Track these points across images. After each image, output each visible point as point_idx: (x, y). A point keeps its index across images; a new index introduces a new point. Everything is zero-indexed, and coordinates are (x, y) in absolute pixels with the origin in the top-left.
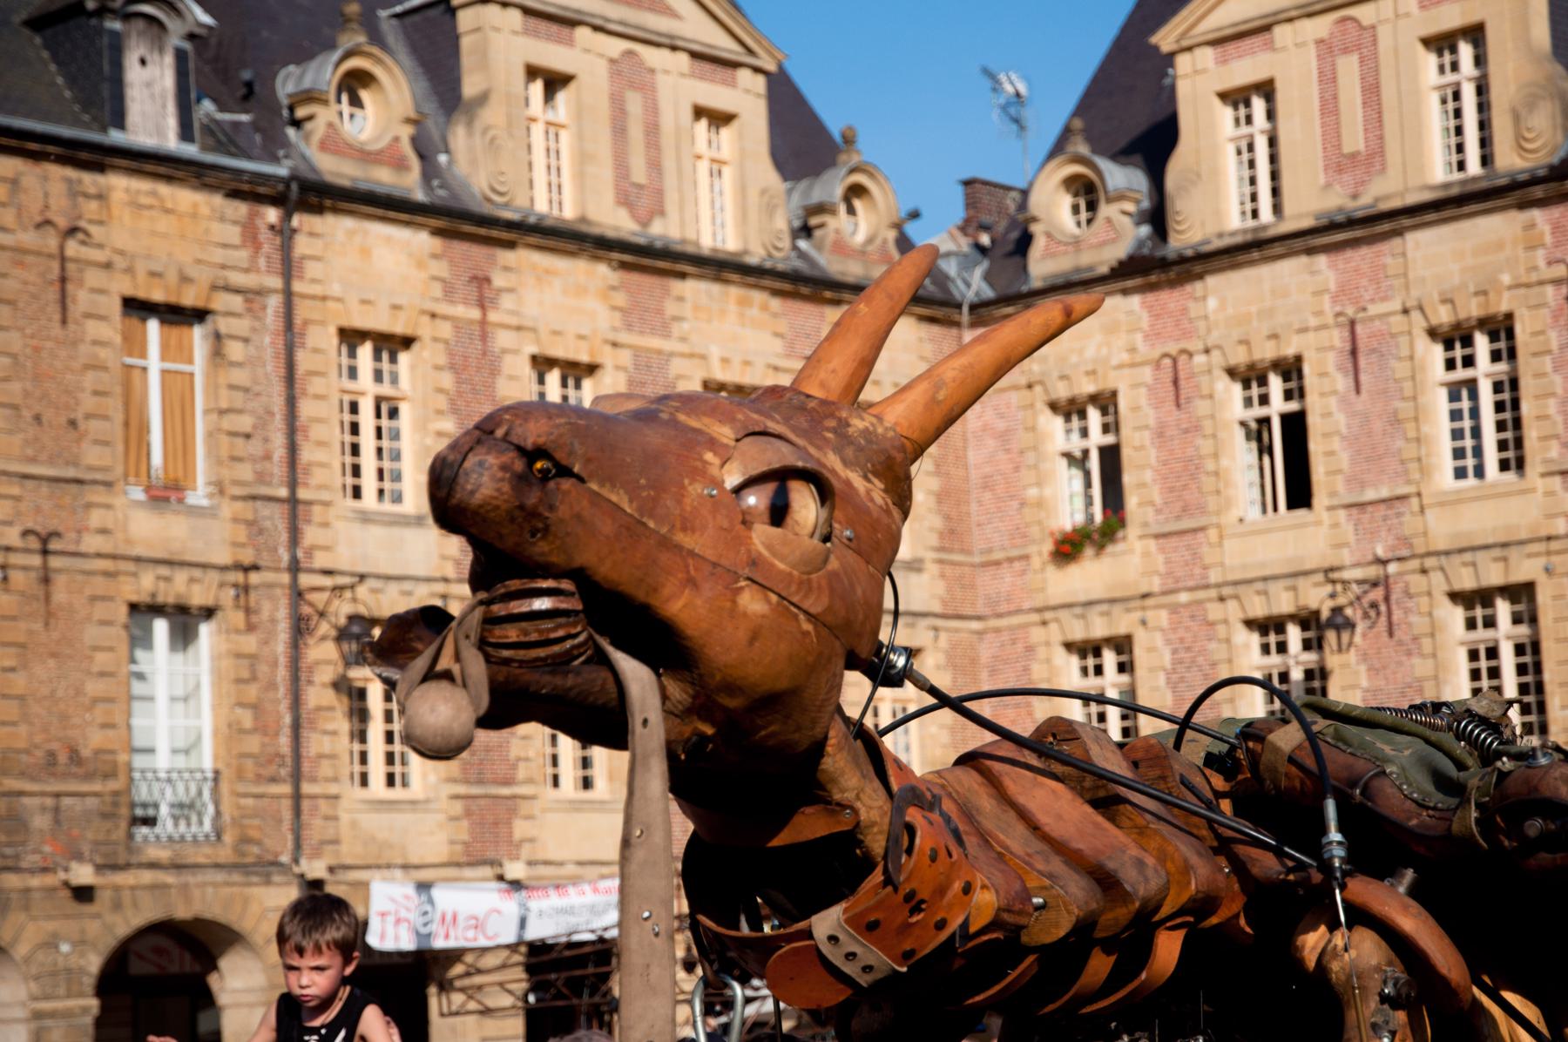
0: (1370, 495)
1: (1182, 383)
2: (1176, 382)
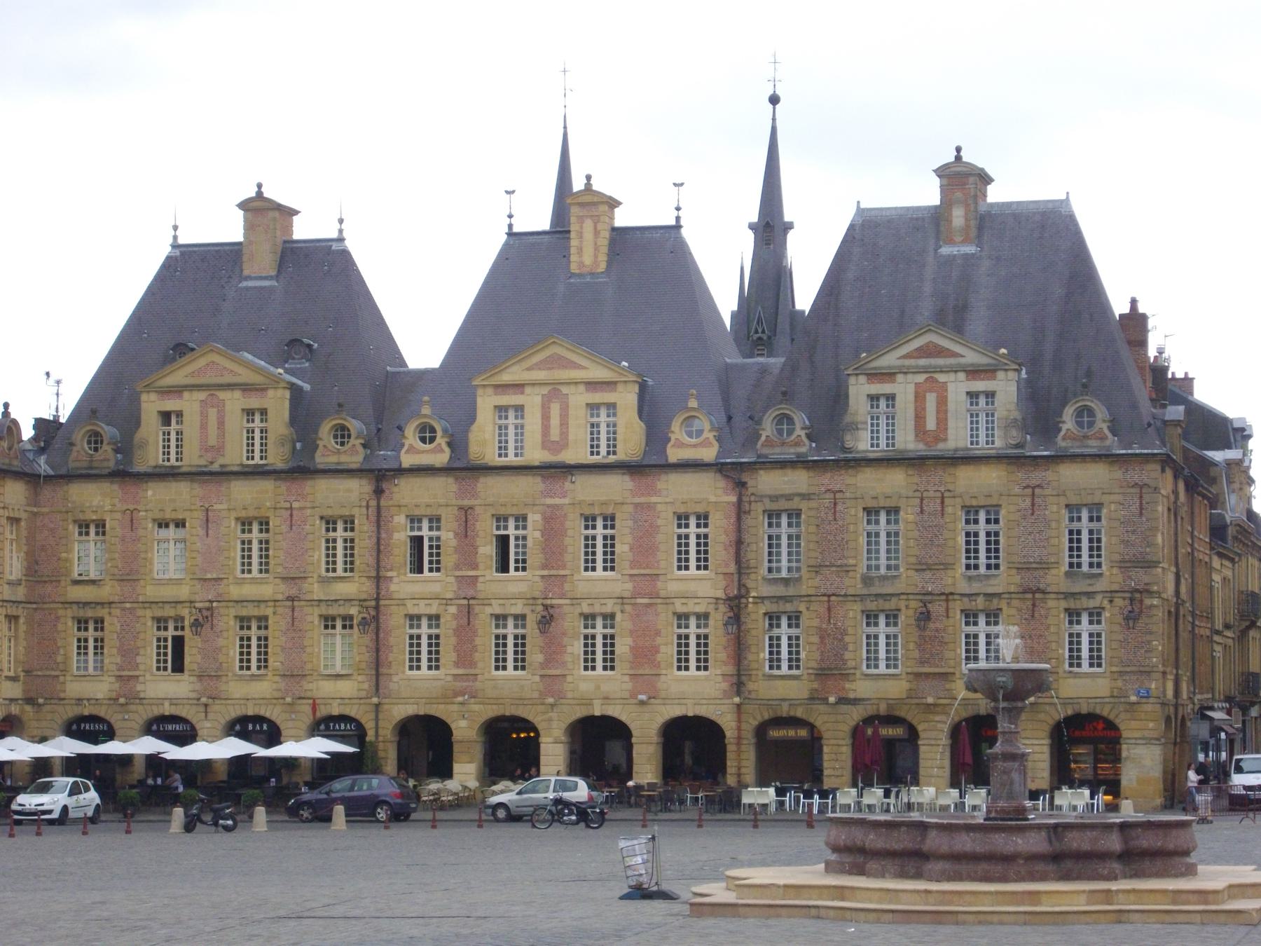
0: (209, 576)
1: (134, 521)
2: (132, 520)
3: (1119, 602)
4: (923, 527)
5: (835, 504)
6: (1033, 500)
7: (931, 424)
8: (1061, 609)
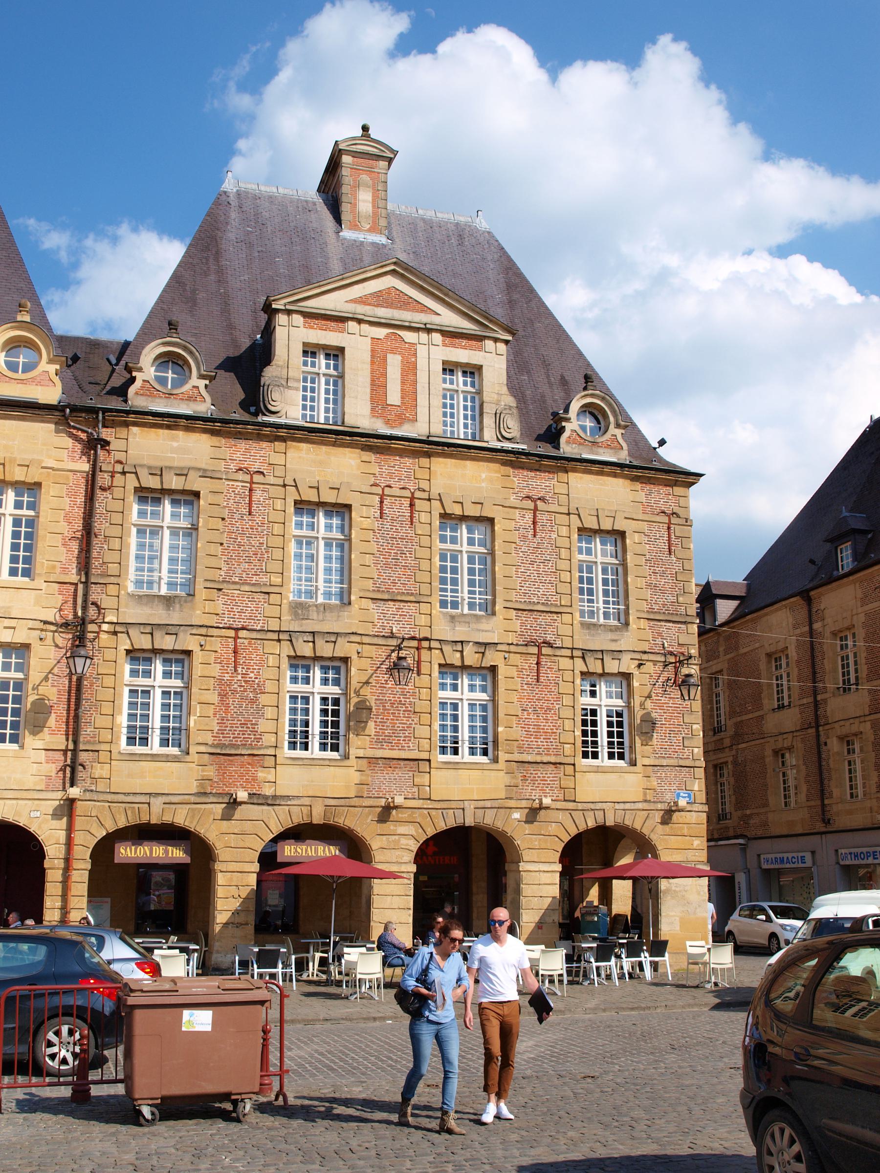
3: (649, 667)
4: (383, 538)
5: (251, 490)
6: (535, 517)
7: (394, 396)
8: (577, 672)
